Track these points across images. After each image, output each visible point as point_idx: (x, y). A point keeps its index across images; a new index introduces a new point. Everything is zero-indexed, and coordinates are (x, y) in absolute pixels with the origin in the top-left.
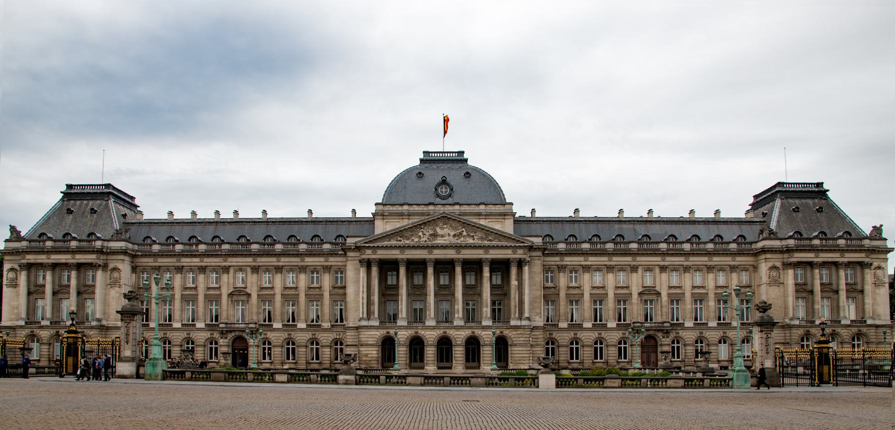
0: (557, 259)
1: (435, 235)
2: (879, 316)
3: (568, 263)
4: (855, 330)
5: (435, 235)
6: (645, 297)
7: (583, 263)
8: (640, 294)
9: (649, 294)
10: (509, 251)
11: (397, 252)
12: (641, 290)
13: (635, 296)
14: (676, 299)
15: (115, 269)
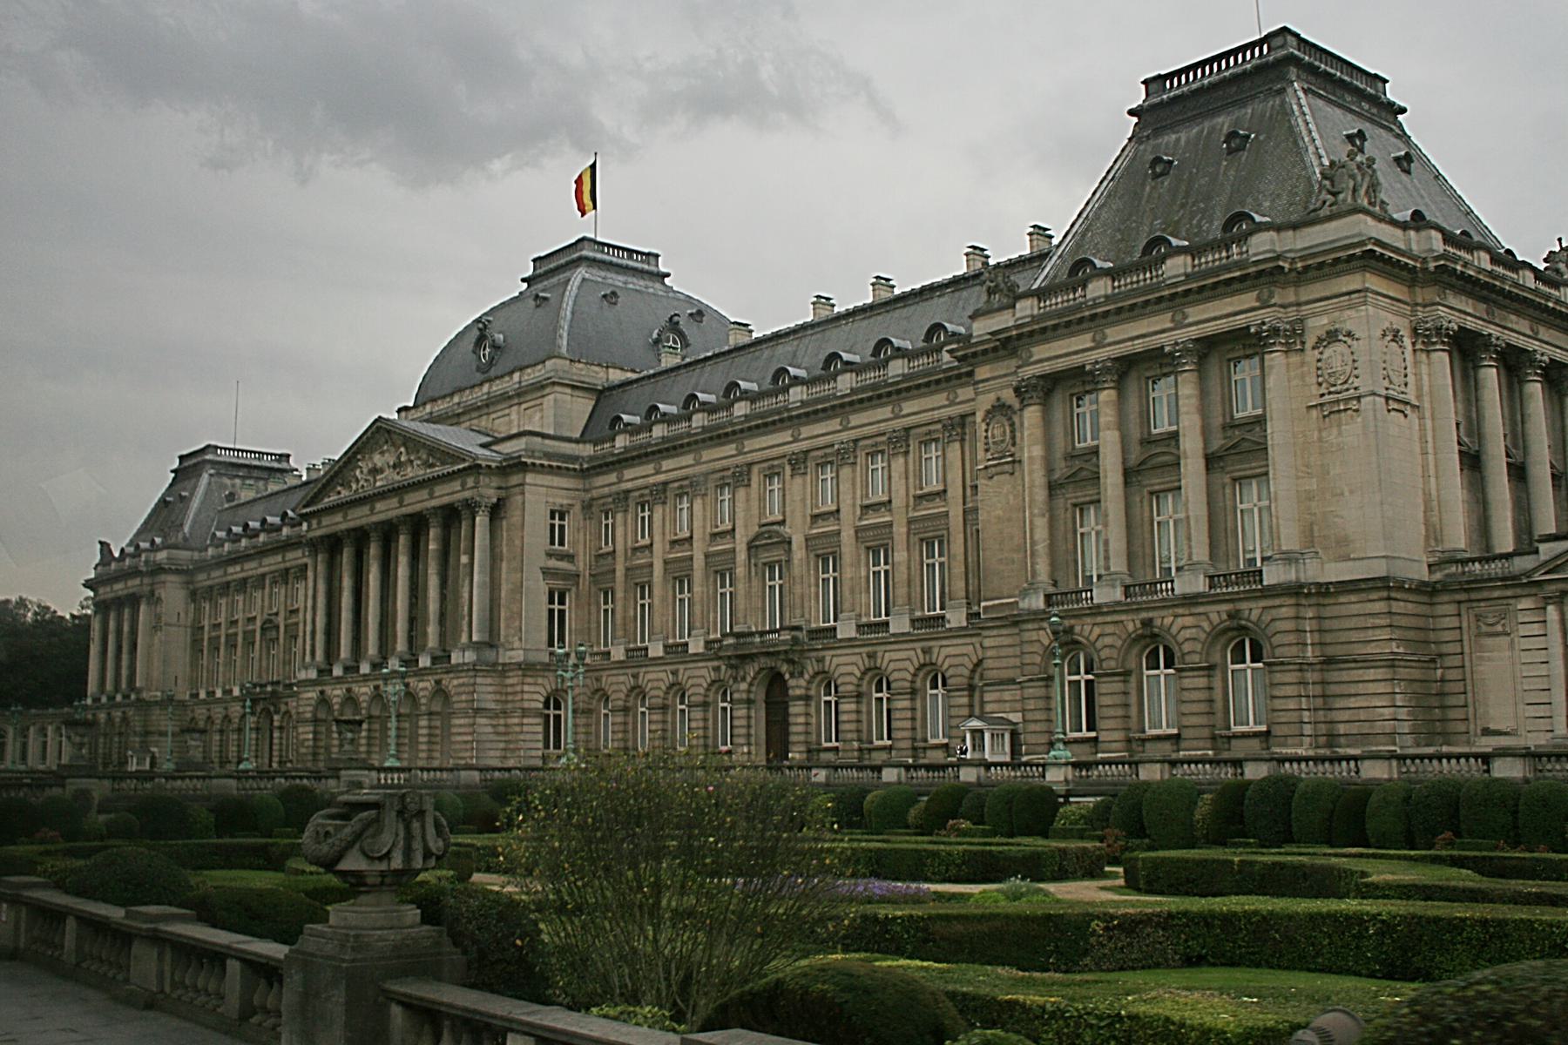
0: (613, 477)
1: (375, 471)
2: (1343, 541)
3: (629, 485)
4: (1217, 614)
5: (375, 471)
6: (765, 556)
7: (651, 480)
8: (751, 547)
9: (770, 540)
10: (456, 485)
11: (338, 518)
12: (752, 534)
13: (742, 556)
14: (825, 553)
15: (159, 599)
